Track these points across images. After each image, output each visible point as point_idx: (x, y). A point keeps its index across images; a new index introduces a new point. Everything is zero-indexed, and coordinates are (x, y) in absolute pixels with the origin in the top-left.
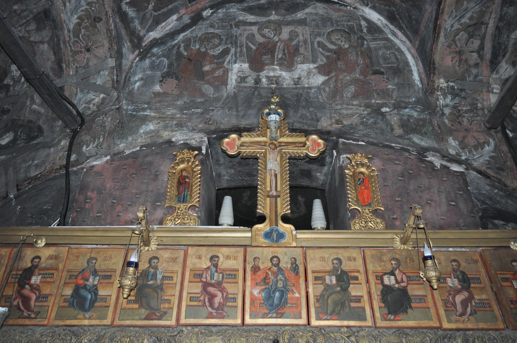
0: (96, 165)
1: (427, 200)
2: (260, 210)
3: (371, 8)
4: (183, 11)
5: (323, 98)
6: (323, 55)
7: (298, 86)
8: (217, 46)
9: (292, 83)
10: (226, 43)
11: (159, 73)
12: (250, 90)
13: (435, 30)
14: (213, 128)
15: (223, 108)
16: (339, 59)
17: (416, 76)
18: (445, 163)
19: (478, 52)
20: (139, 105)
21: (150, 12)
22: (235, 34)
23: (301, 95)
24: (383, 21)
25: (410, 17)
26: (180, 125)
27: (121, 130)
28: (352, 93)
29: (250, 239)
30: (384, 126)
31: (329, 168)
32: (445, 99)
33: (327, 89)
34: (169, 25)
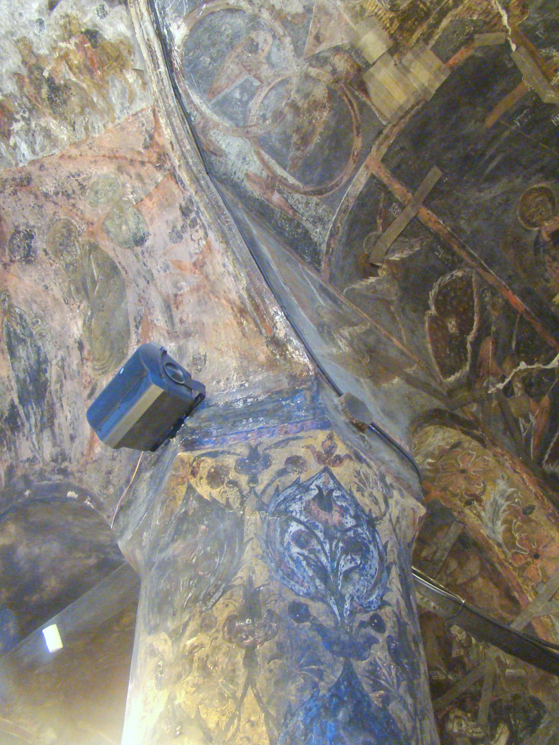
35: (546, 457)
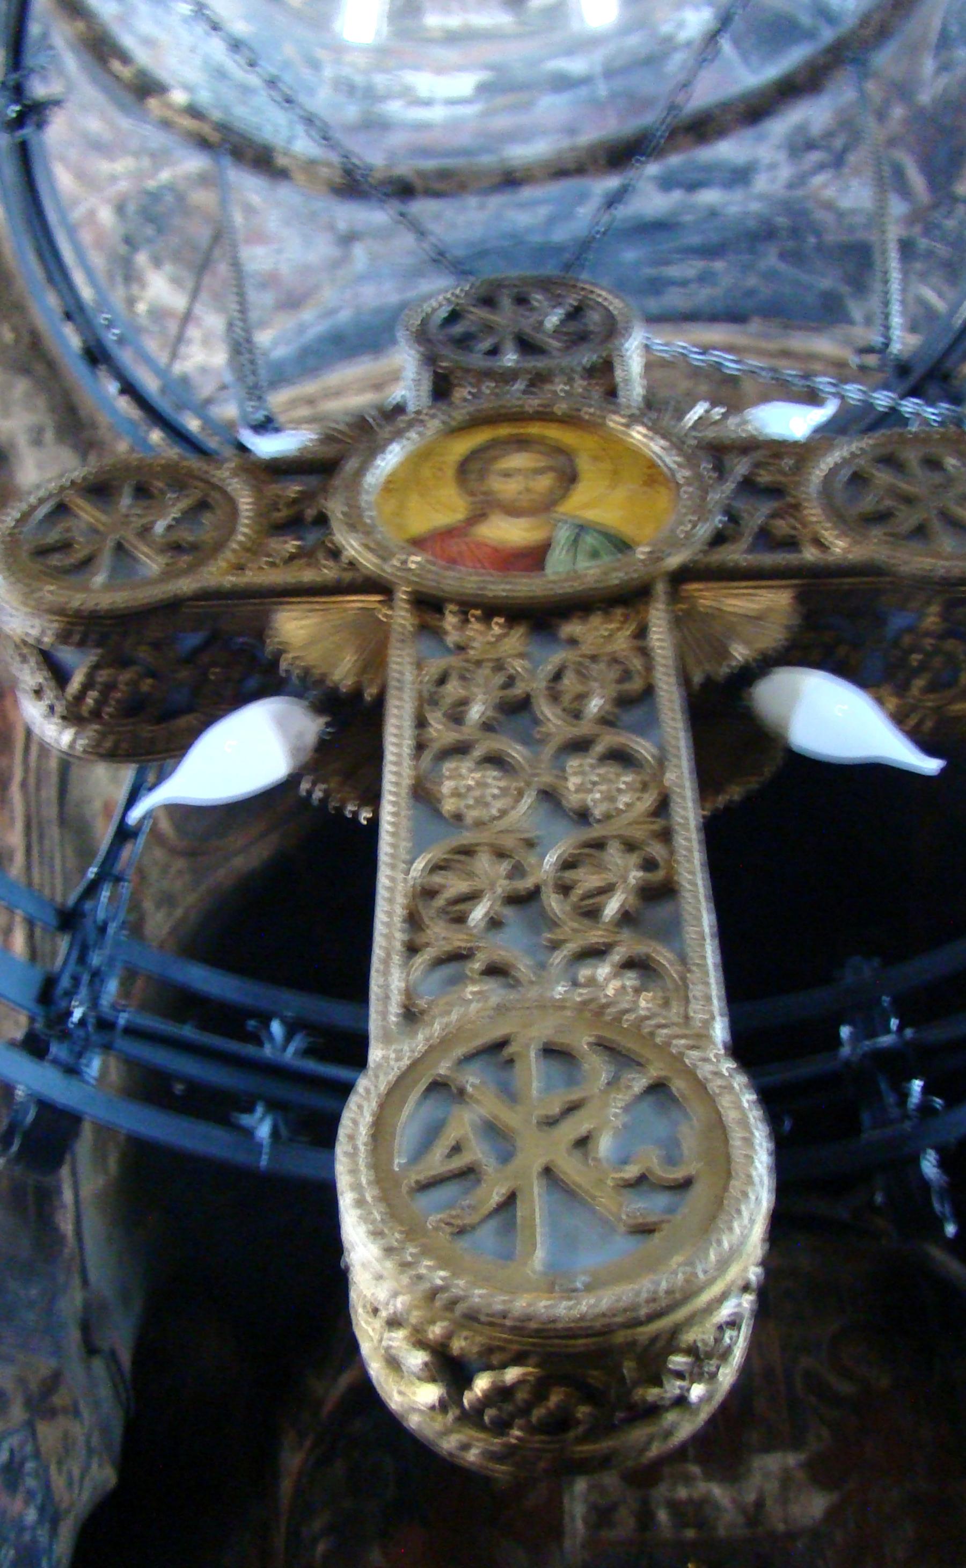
9: (740, 1520)
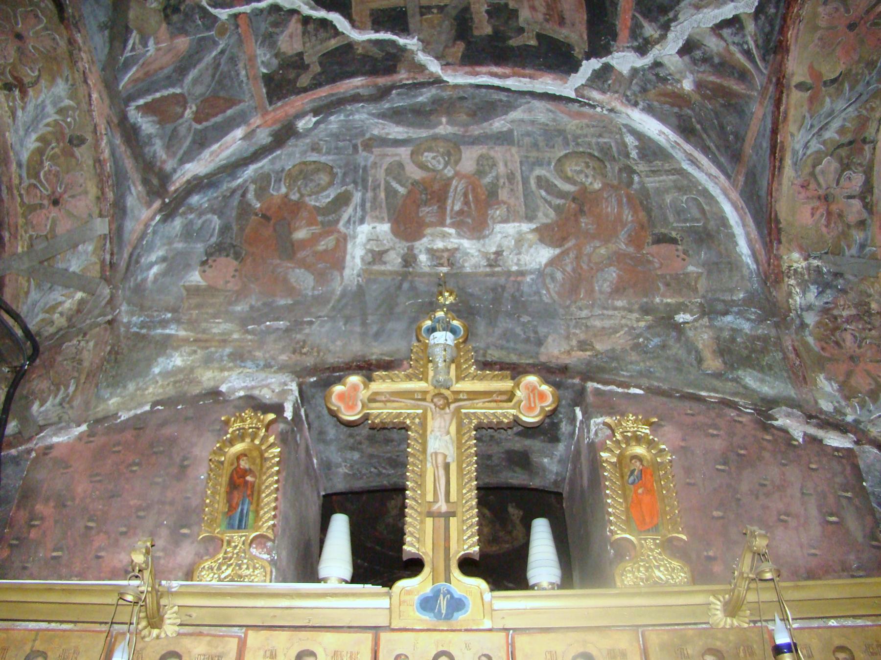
0: (58, 443)
1: (779, 514)
2: (410, 548)
3: (643, 110)
4: (256, 121)
5: (550, 293)
6: (550, 204)
7: (497, 269)
8: (324, 189)
9: (484, 263)
10: (343, 183)
11: (200, 247)
12: (393, 279)
13: (773, 152)
14: (309, 361)
15: (332, 319)
16: (581, 211)
17: (743, 247)
18: (812, 431)
19: (862, 198)
20: (155, 314)
21: (187, 124)
22: (362, 164)
23: (503, 288)
24: (670, 137)
25: (722, 127)
26: (239, 357)
27: (113, 367)
28: (611, 282)
29: (387, 611)
30: (682, 353)
31: (568, 447)
32: (804, 293)
33: (559, 275)
34: (227, 148)
35: (141, 102)
